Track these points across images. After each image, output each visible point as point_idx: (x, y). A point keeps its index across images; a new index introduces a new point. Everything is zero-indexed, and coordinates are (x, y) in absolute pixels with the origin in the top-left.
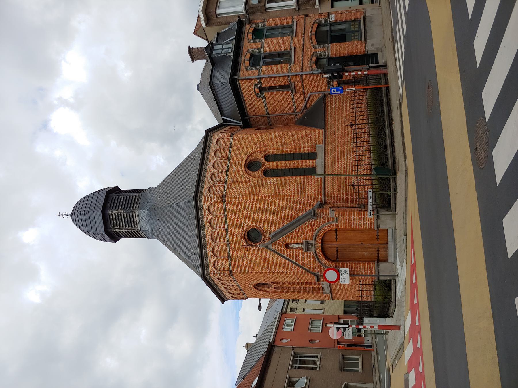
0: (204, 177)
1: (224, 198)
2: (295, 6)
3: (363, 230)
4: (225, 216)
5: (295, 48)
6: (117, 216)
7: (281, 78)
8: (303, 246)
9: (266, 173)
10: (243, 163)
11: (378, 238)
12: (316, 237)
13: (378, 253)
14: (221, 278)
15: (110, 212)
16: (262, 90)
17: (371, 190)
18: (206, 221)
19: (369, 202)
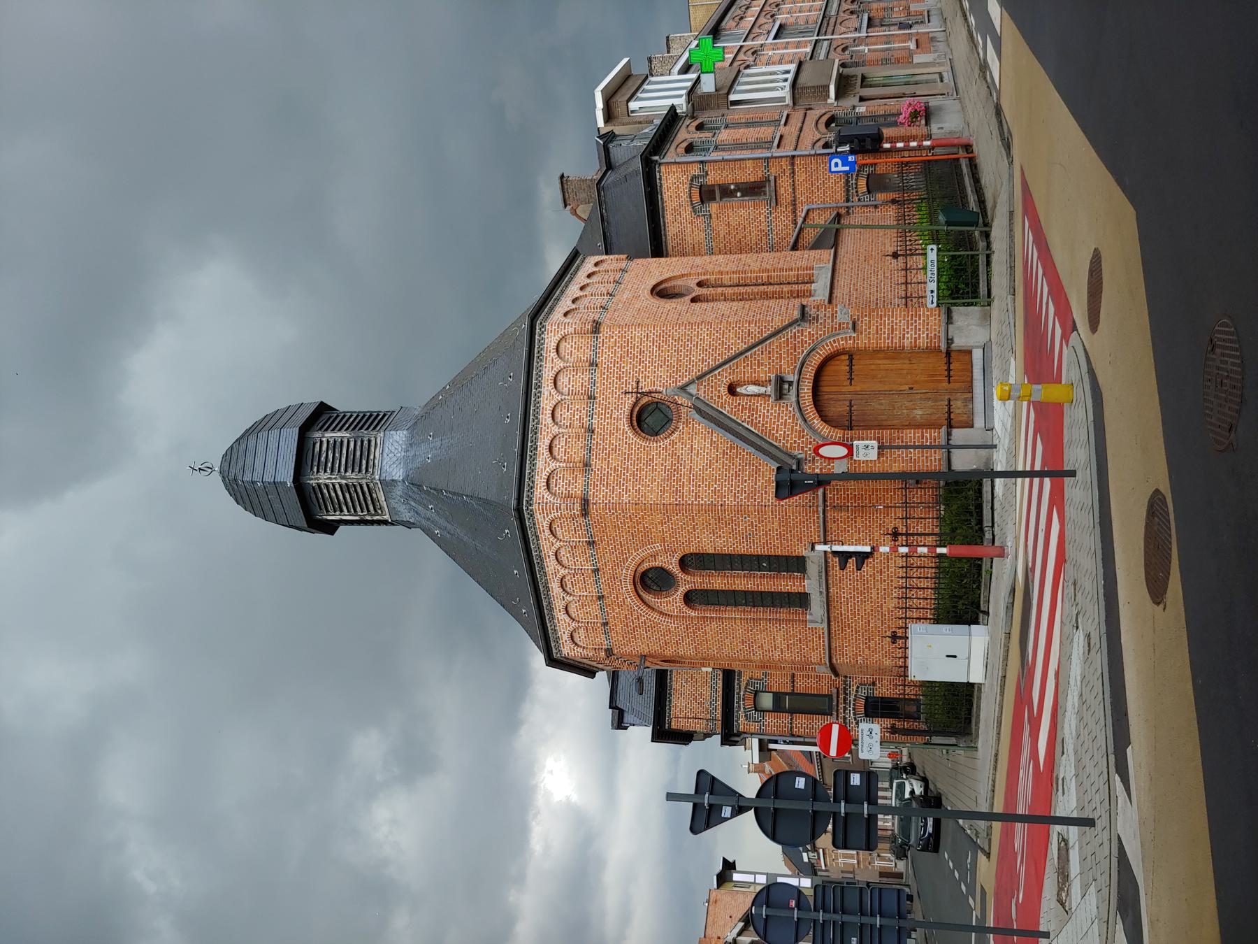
0: (558, 299)
1: (596, 328)
2: (788, 101)
3: (915, 353)
4: (593, 364)
5: (781, 137)
6: (331, 446)
7: (749, 164)
8: (769, 389)
9: (693, 300)
10: (650, 287)
11: (949, 376)
12: (802, 365)
13: (949, 413)
14: (559, 533)
15: (317, 435)
16: (707, 194)
17: (934, 247)
18: (548, 375)
19: (929, 273)
